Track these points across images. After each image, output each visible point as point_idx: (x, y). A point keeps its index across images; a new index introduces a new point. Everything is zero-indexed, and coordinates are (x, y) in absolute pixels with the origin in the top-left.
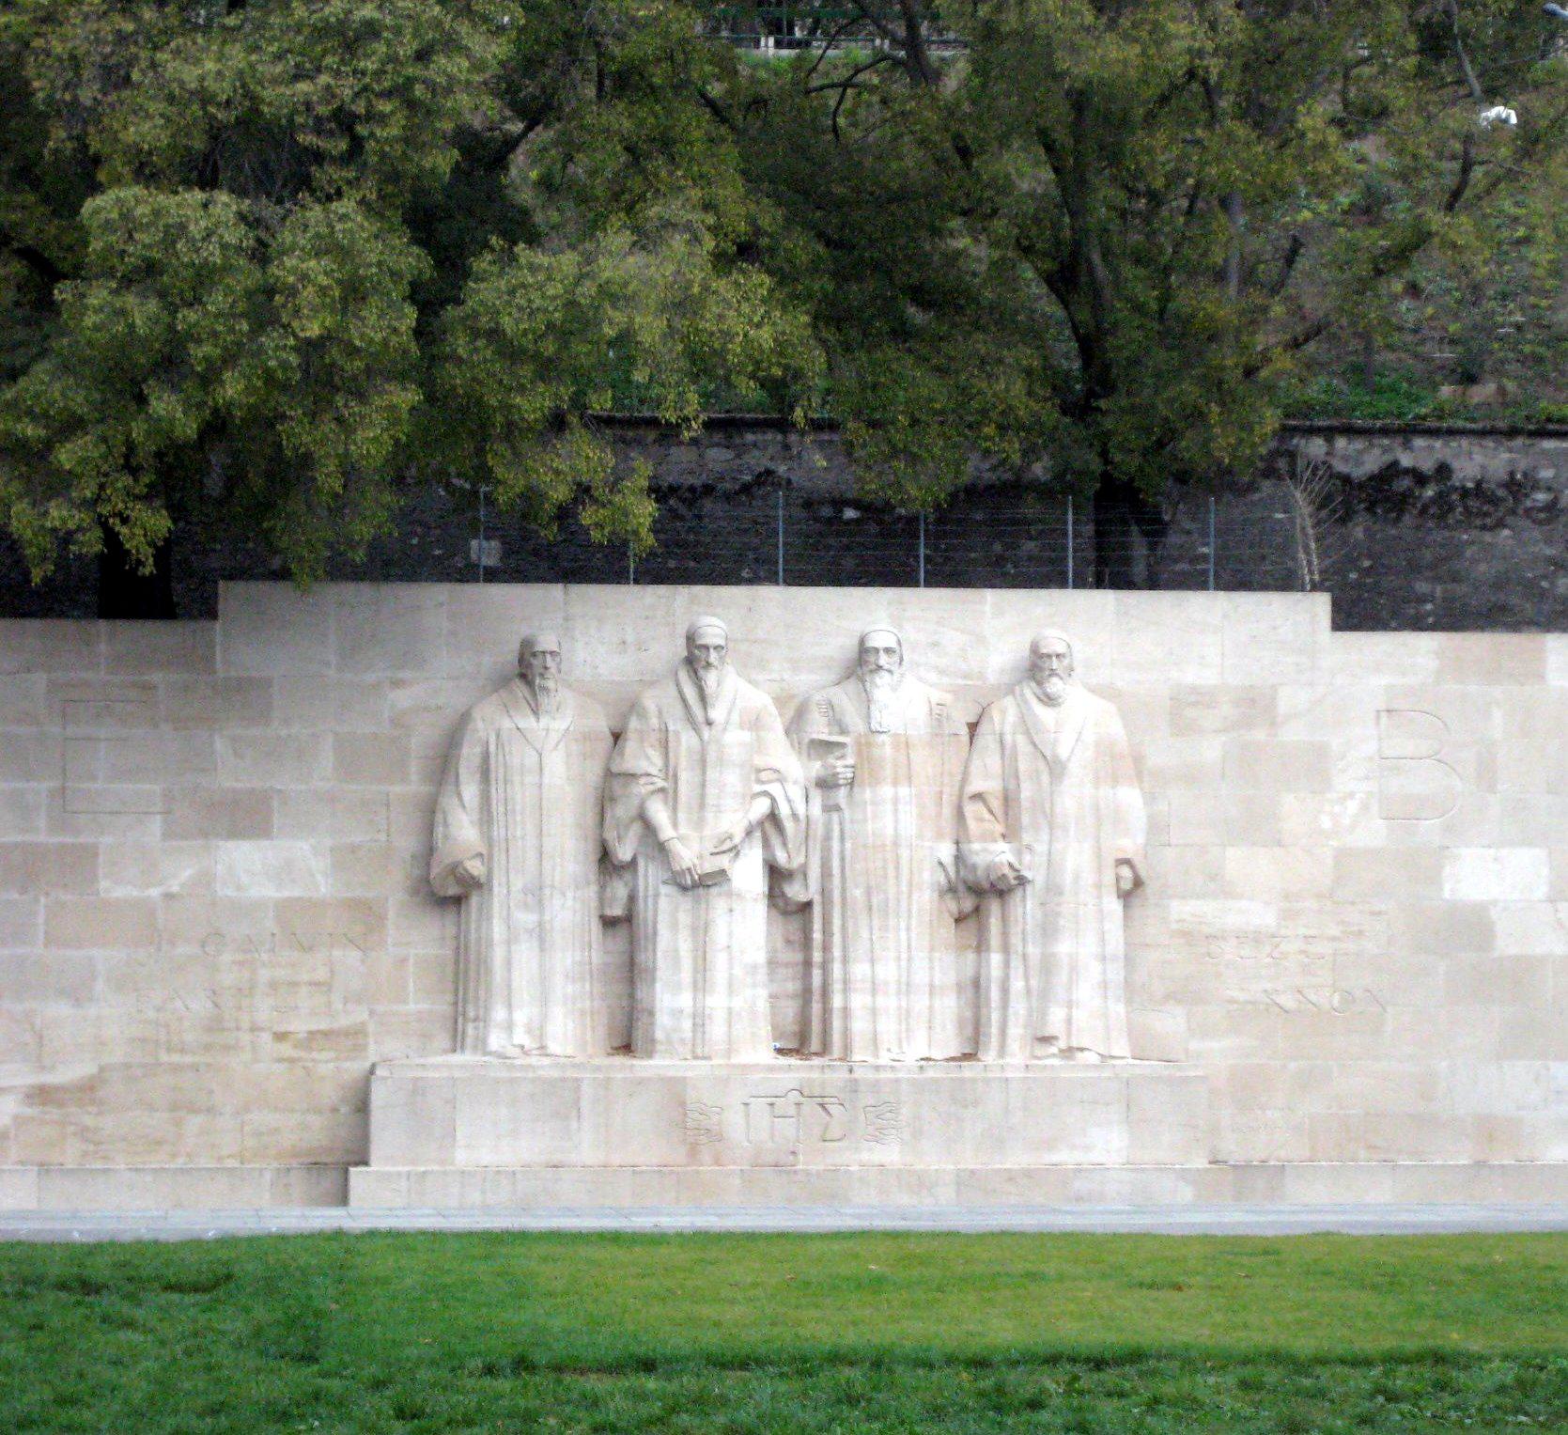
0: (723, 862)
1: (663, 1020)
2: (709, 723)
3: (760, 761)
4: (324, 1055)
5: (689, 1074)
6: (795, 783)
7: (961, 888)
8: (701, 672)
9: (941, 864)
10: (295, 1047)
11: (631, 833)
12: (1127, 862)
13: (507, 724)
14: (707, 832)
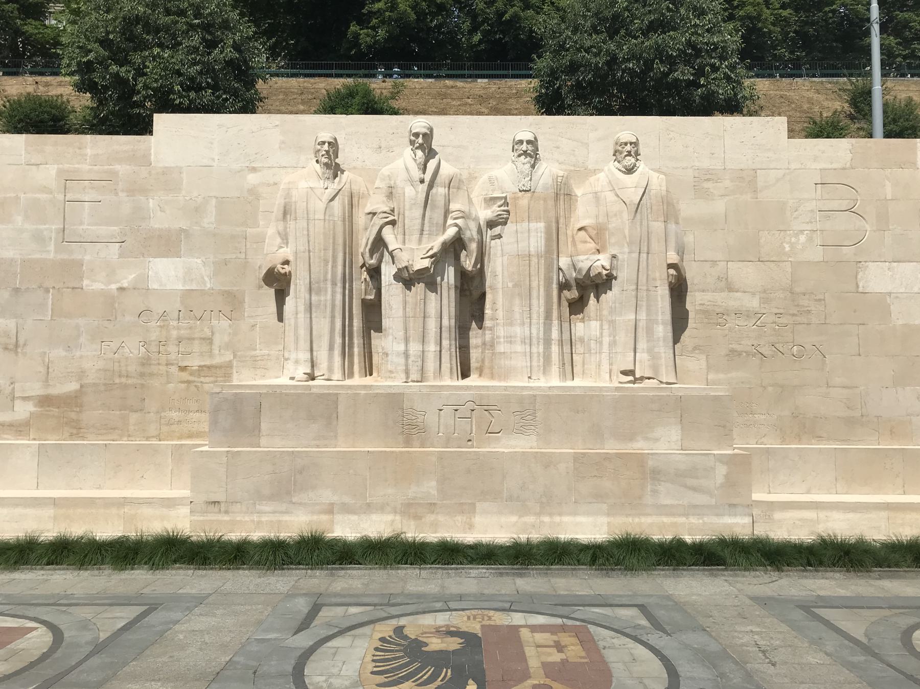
4: (208, 379)
5: (407, 391)
7: (573, 283)
9: (560, 269)
10: (191, 375)
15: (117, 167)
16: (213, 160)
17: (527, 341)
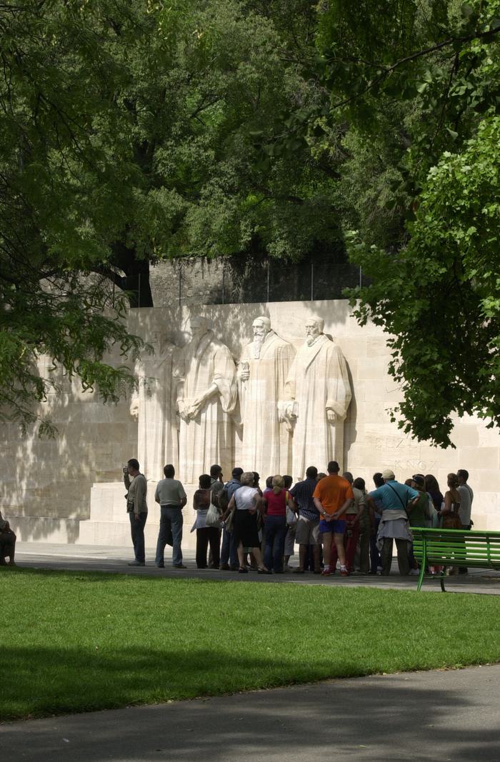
6: (228, 379)
12: (330, 409)
17: (254, 458)
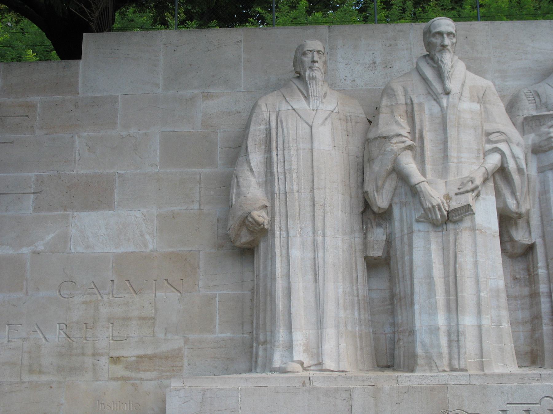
0: (469, 198)
1: (422, 335)
2: (447, 93)
3: (488, 127)
4: (148, 375)
6: (518, 145)
8: (438, 56)
10: (127, 368)
11: (387, 185)
13: (284, 106)
14: (451, 178)
15: (36, 99)
16: (158, 85)
